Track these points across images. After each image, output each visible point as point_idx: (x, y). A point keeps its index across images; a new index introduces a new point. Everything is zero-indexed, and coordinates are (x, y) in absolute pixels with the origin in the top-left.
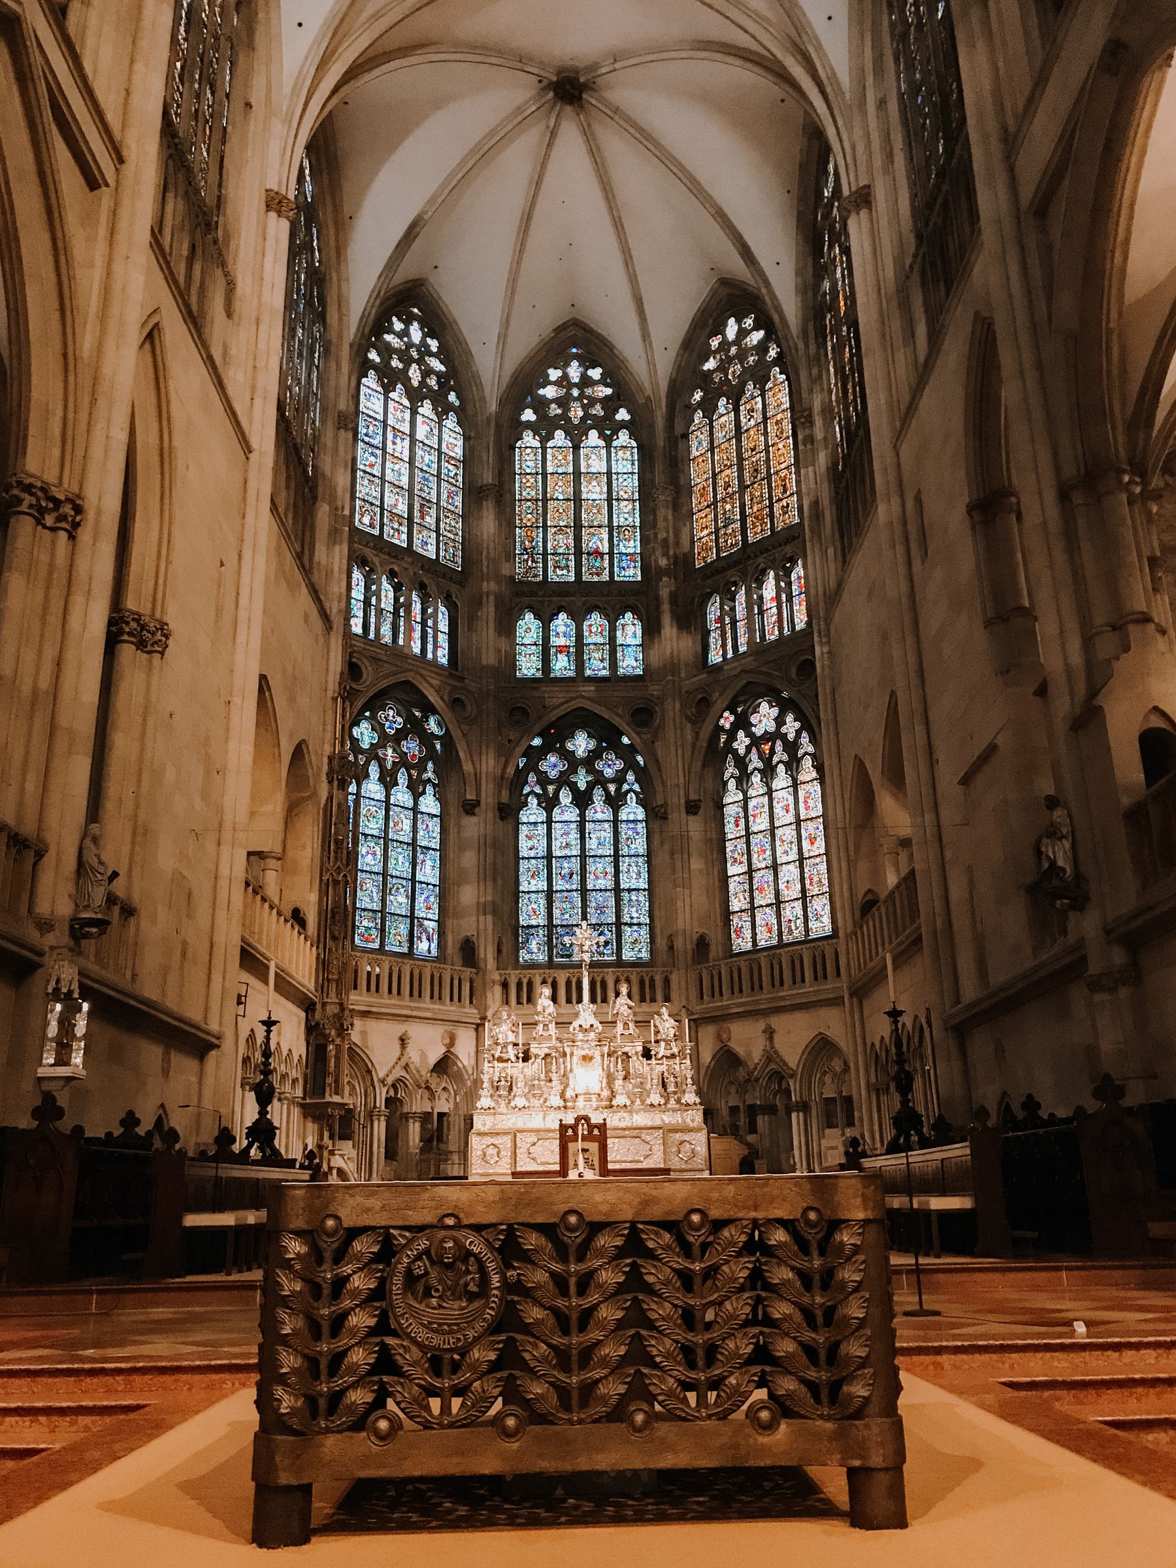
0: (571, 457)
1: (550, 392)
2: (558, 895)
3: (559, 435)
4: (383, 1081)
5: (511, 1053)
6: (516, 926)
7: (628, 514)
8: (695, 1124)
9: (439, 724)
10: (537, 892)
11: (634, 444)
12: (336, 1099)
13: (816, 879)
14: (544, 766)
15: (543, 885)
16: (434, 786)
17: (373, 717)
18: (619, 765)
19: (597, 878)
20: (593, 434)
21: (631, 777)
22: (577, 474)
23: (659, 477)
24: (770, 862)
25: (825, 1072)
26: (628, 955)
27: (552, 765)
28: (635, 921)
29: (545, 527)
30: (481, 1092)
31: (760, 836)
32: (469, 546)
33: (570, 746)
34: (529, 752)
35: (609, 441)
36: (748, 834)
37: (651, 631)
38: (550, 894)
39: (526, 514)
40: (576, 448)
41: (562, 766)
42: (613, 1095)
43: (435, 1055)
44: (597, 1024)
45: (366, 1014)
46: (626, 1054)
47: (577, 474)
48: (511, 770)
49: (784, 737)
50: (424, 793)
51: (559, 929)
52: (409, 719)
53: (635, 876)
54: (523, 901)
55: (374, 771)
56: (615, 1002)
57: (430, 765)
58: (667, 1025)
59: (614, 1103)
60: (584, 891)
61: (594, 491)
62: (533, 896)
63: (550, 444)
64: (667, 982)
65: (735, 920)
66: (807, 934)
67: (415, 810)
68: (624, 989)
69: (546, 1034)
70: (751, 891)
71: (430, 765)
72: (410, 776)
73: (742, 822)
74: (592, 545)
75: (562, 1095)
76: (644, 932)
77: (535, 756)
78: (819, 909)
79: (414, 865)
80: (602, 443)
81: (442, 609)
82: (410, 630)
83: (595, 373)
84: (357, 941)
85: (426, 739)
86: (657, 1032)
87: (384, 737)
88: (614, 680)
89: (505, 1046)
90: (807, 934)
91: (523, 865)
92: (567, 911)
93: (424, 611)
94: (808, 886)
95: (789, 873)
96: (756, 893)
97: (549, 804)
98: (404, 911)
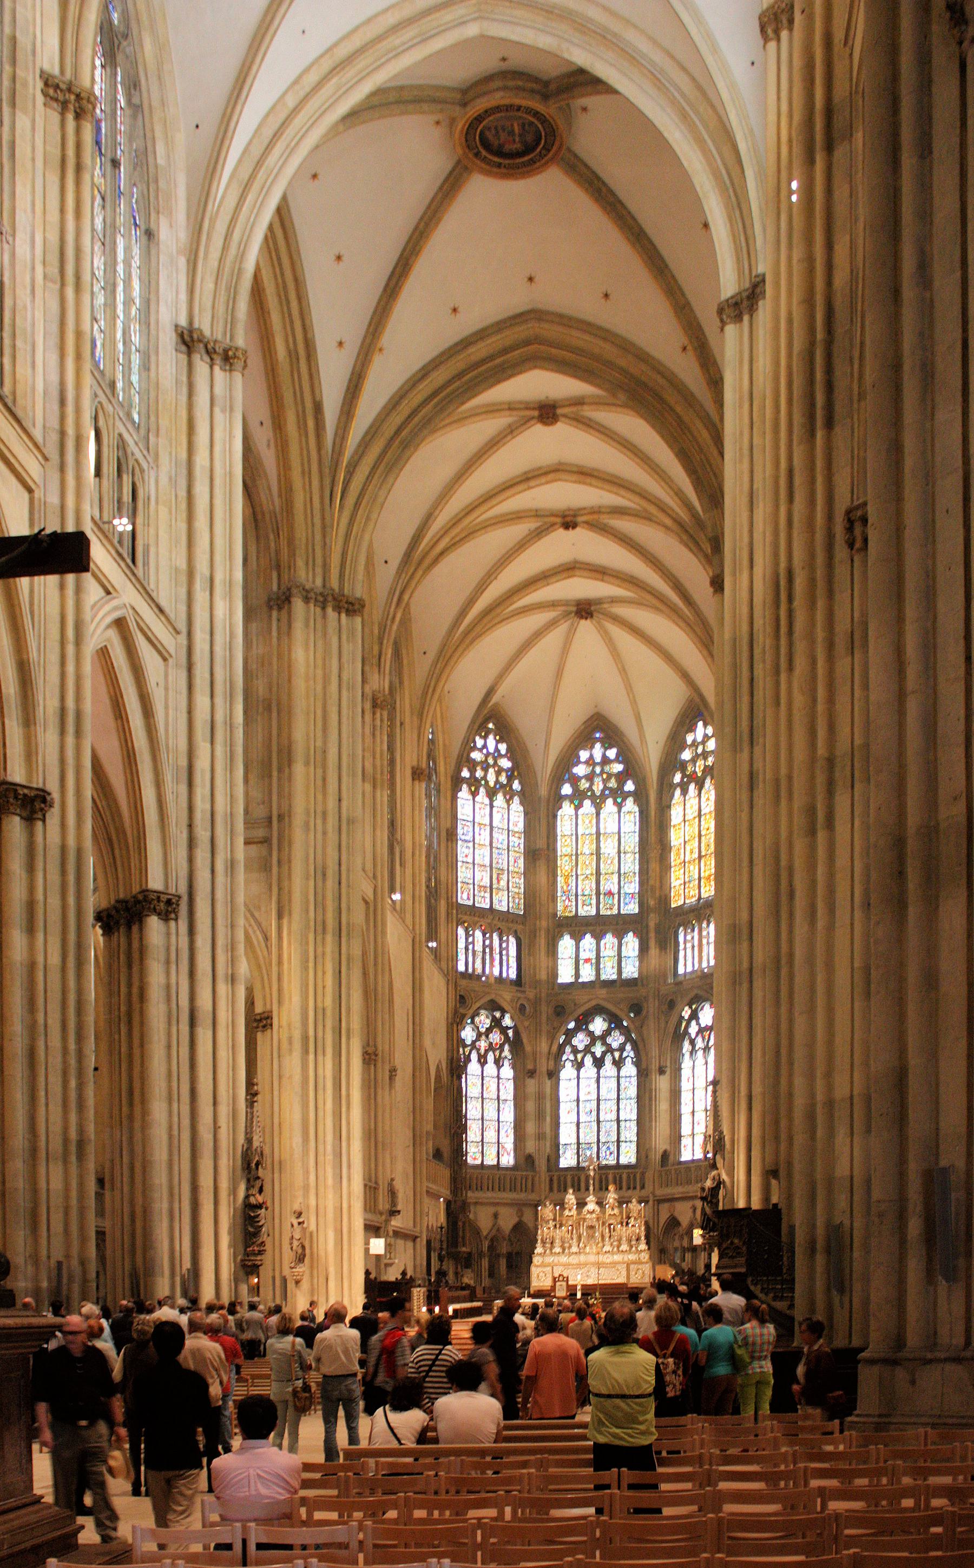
0: (594, 821)
1: (580, 770)
3: (587, 803)
5: (551, 1224)
7: (631, 864)
9: (512, 1018)
11: (636, 809)
12: (464, 1249)
17: (473, 1022)
20: (610, 801)
22: (598, 834)
23: (653, 838)
29: (577, 876)
32: (530, 896)
35: (620, 806)
37: (644, 949)
39: (564, 865)
40: (598, 814)
43: (514, 1221)
44: (597, 1208)
45: (476, 1203)
47: (598, 834)
52: (494, 1018)
55: (474, 1056)
57: (507, 1047)
61: (609, 847)
63: (581, 811)
67: (498, 1077)
71: (507, 1047)
74: (607, 888)
77: (570, 1034)
80: (615, 809)
81: (512, 940)
82: (492, 959)
83: (612, 753)
84: (470, 1161)
85: (504, 1030)
87: (479, 1035)
88: (622, 983)
89: (547, 1222)
93: (501, 945)
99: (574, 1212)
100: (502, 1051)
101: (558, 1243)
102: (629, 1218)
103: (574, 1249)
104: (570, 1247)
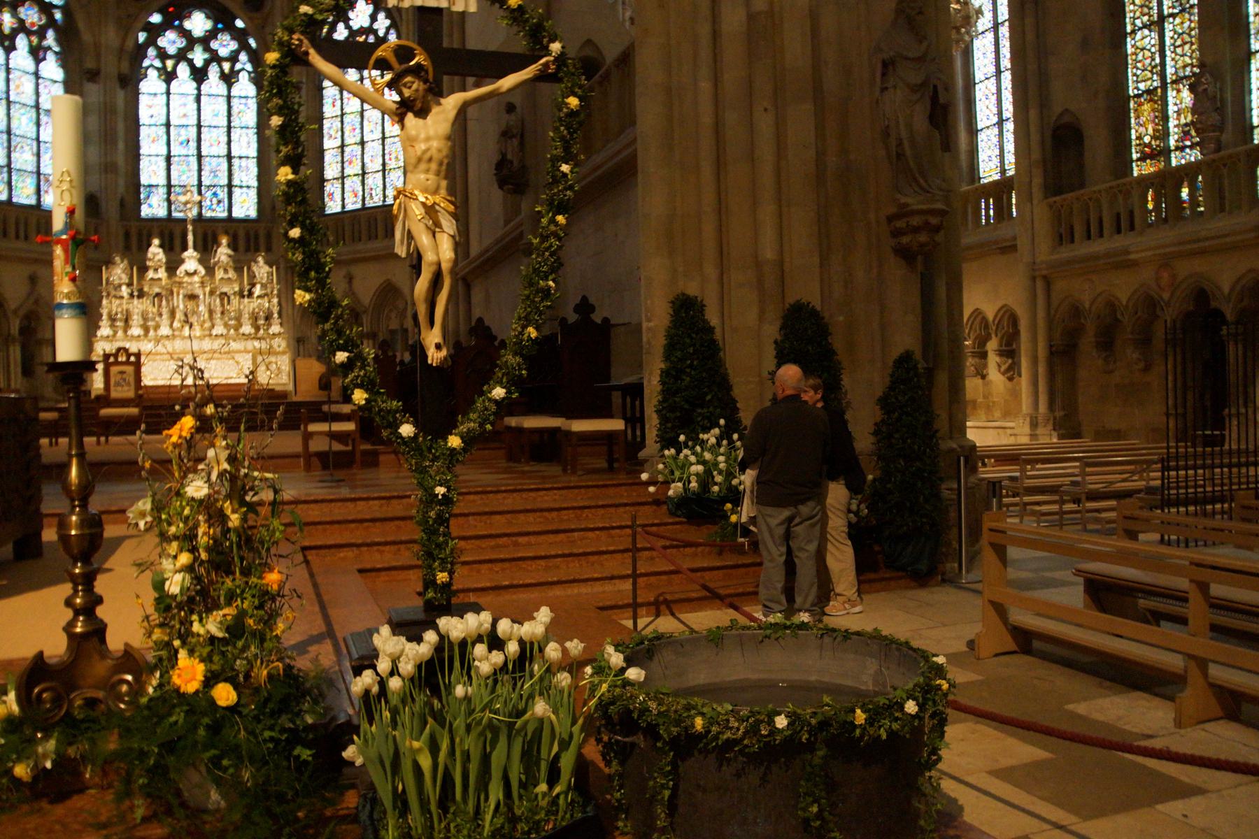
2: (176, 159)
4: (15, 312)
5: (125, 291)
6: (137, 185)
8: (281, 349)
10: (157, 156)
13: (393, 156)
14: (162, 42)
15: (165, 152)
16: (56, 53)
18: (234, 45)
19: (211, 145)
21: (243, 57)
24: (358, 139)
25: (391, 310)
26: (238, 213)
27: (170, 41)
28: (244, 184)
30: (101, 324)
31: (352, 116)
33: (187, 25)
34: (149, 28)
36: (342, 115)
38: (168, 158)
41: (181, 43)
42: (213, 326)
46: (225, 294)
48: (130, 44)
49: (375, 32)
50: (44, 59)
51: (177, 189)
53: (246, 144)
54: (144, 164)
56: (216, 251)
57: (50, 34)
58: (262, 271)
59: (214, 332)
60: (200, 157)
62: (152, 158)
64: (269, 236)
65: (328, 188)
66: (384, 201)
67: (37, 75)
68: (224, 241)
69: (156, 276)
70: (343, 162)
71: (50, 34)
72: (30, 42)
73: (338, 103)
75: (171, 326)
76: (253, 194)
77: (155, 32)
78: (395, 180)
79: (38, 125)
86: (252, 276)
89: (120, 286)
90: (384, 201)
91: (144, 132)
92: (184, 174)
94: (387, 161)
95: (373, 149)
96: (346, 165)
97: (169, 77)
98: (31, 167)
99: (162, 274)
100: (42, 36)
101: (136, 320)
102: (253, 285)
103: (165, 330)
104: (157, 327)
